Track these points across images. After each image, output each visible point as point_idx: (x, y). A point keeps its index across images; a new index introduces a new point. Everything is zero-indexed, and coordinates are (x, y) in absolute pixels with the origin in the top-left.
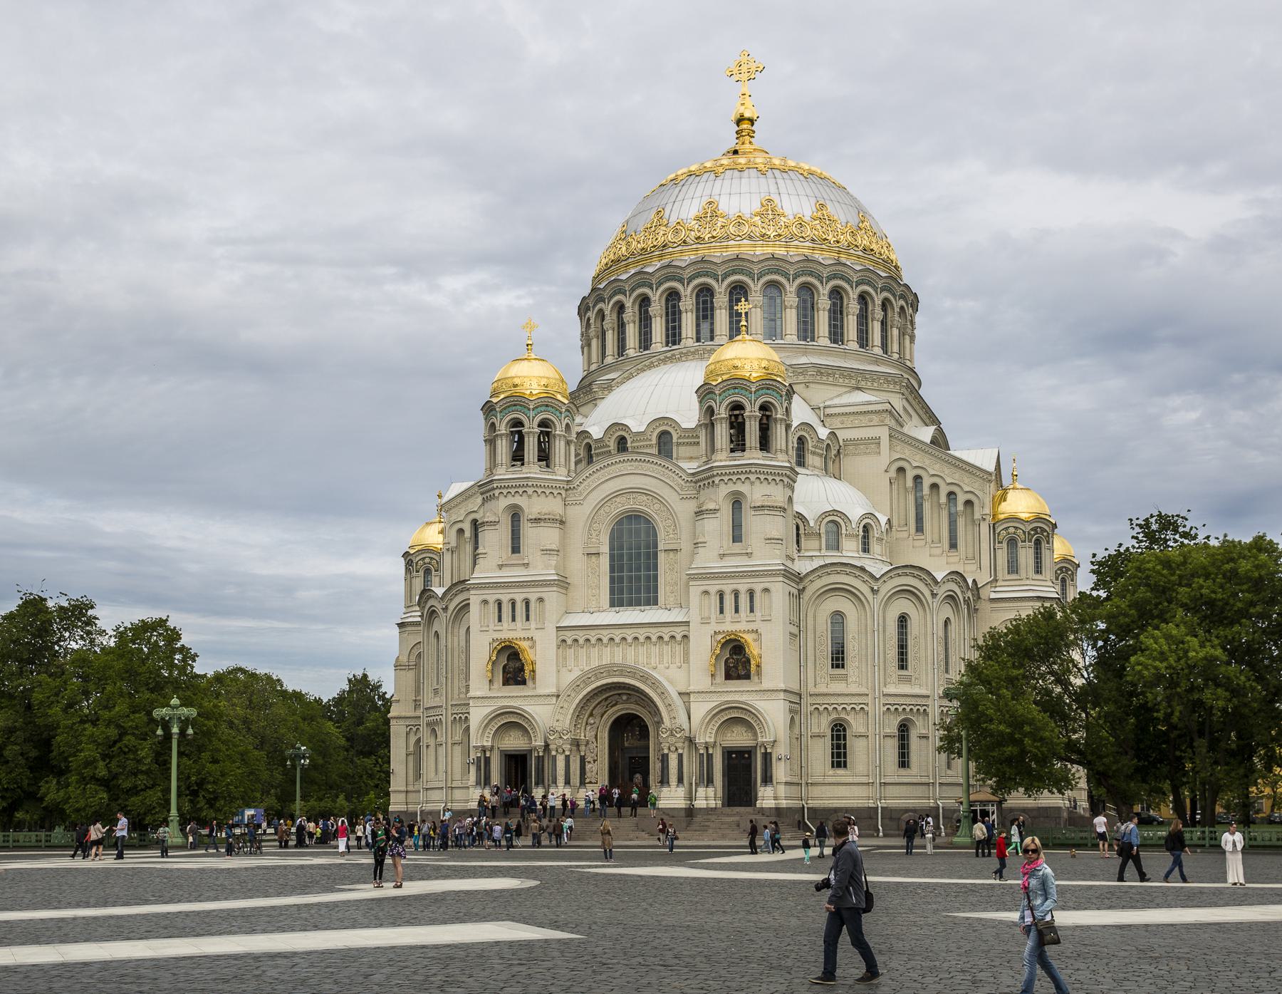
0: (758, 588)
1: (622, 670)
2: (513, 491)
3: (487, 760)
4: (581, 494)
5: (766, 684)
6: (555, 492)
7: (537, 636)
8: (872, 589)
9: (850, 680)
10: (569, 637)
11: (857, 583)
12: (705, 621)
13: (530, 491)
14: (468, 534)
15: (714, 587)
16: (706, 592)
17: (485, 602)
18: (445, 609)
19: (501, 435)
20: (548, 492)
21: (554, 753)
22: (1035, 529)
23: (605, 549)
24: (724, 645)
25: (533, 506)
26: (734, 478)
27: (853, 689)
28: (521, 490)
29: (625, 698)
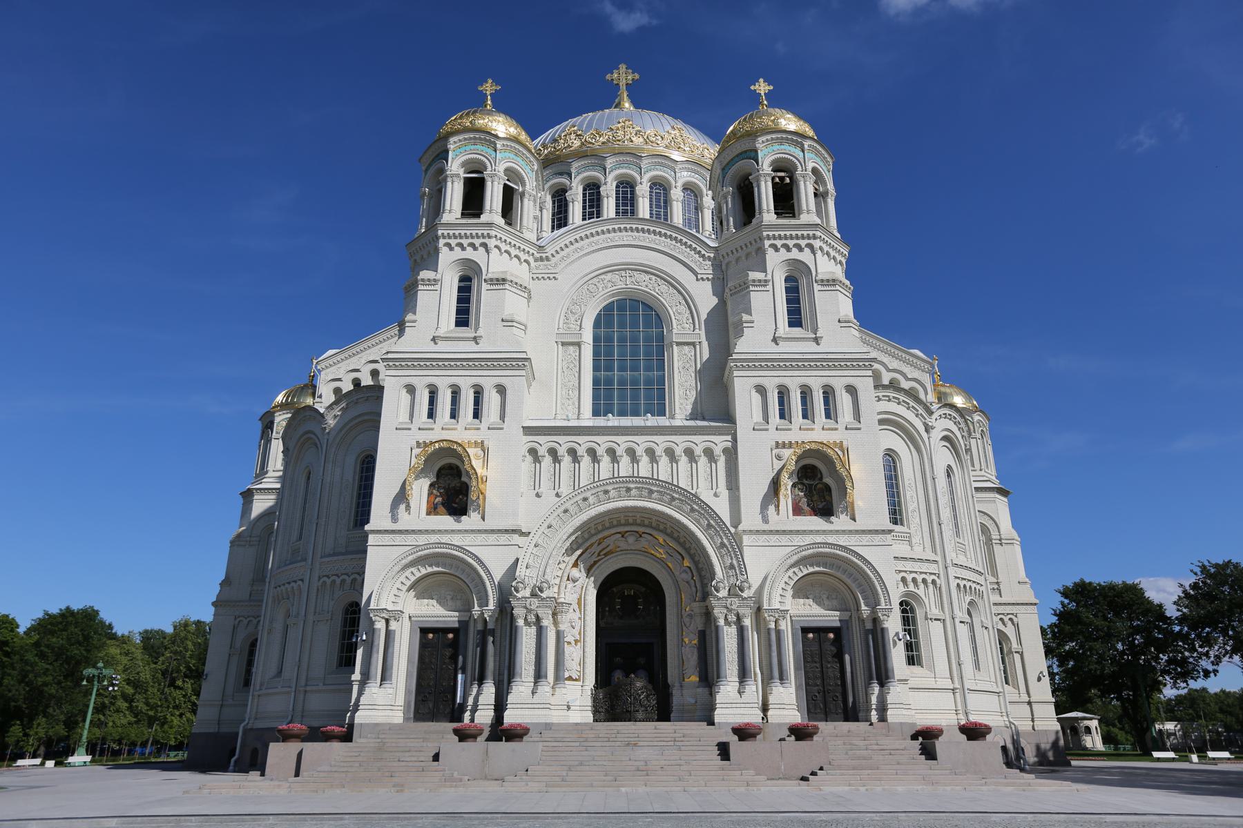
0: (839, 384)
3: (389, 634)
6: (523, 257)
7: (492, 440)
8: (926, 425)
9: (914, 541)
10: (544, 443)
11: (910, 415)
13: (492, 243)
15: (771, 382)
20: (514, 252)
22: (979, 421)
23: (588, 337)
24: (799, 459)
25: (495, 264)
27: (918, 552)
28: (477, 242)
29: (631, 540)
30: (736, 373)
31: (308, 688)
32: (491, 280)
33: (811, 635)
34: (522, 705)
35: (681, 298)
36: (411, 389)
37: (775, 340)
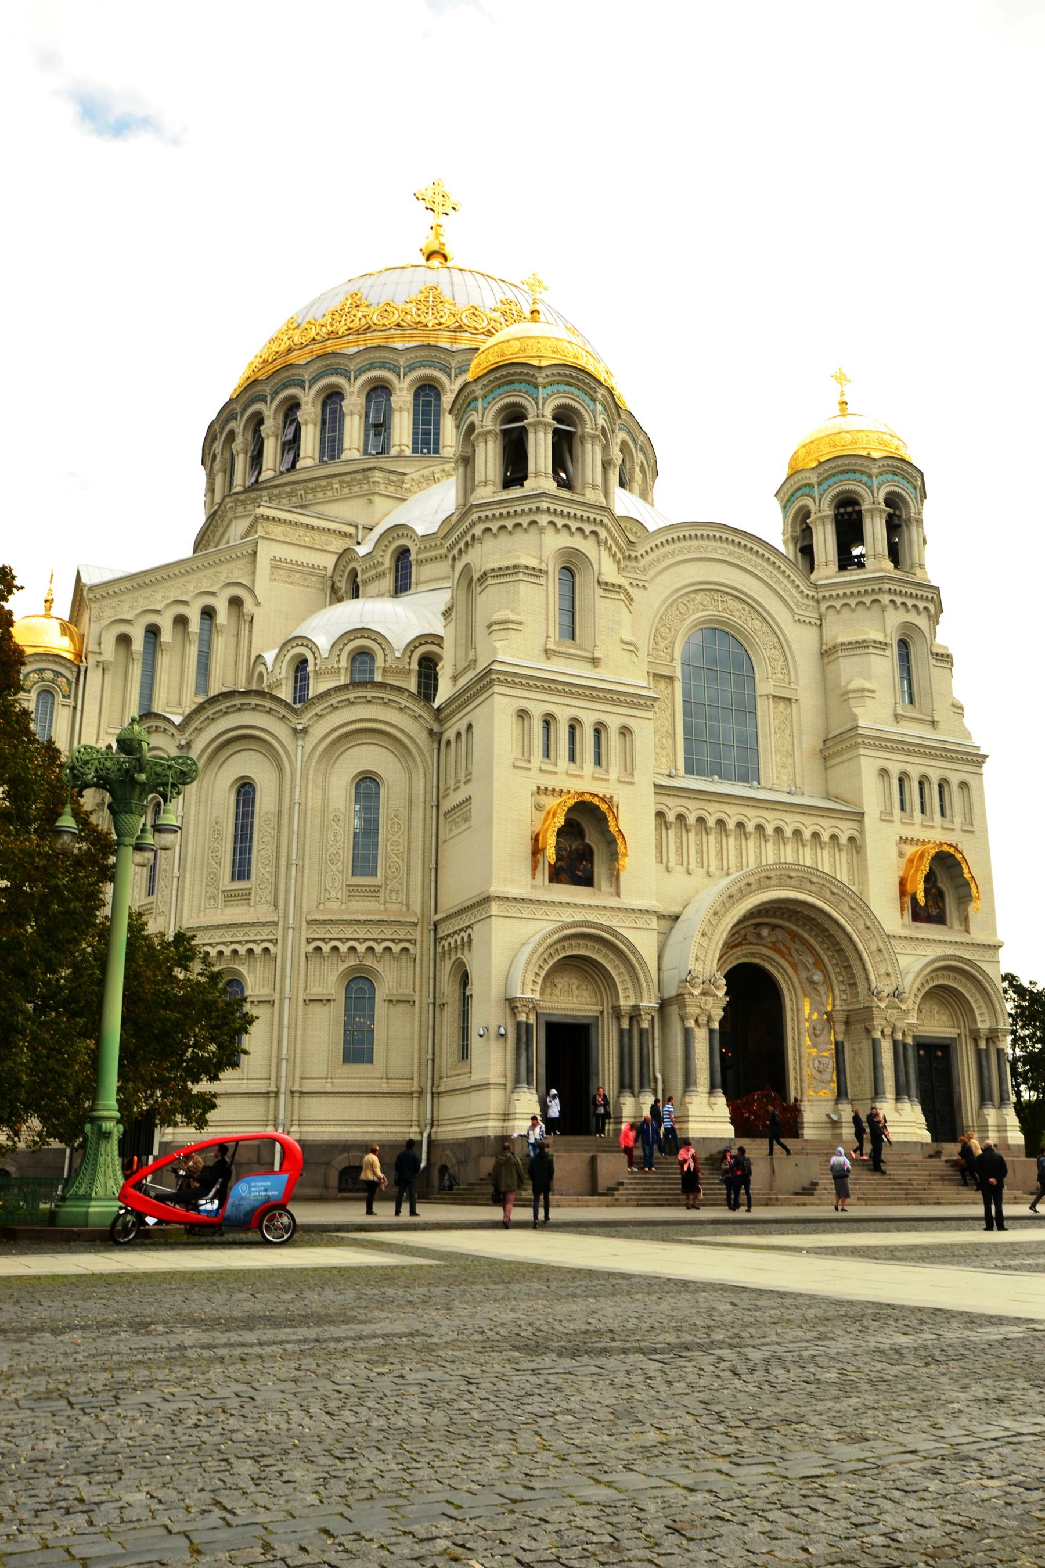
1: (809, 877)
2: (574, 525)
4: (644, 571)
5: (977, 935)
7: (622, 796)
10: (673, 807)
12: (886, 817)
14: (138, 645)
16: (884, 772)
17: (523, 714)
18: (305, 731)
19: (545, 425)
21: (691, 1024)
23: (679, 674)
26: (910, 602)
28: (588, 528)
29: (765, 932)
30: (862, 751)
31: (305, 1090)
32: (606, 584)
33: (922, 1052)
34: (703, 1119)
35: (775, 640)
36: (523, 714)
37: (897, 718)
